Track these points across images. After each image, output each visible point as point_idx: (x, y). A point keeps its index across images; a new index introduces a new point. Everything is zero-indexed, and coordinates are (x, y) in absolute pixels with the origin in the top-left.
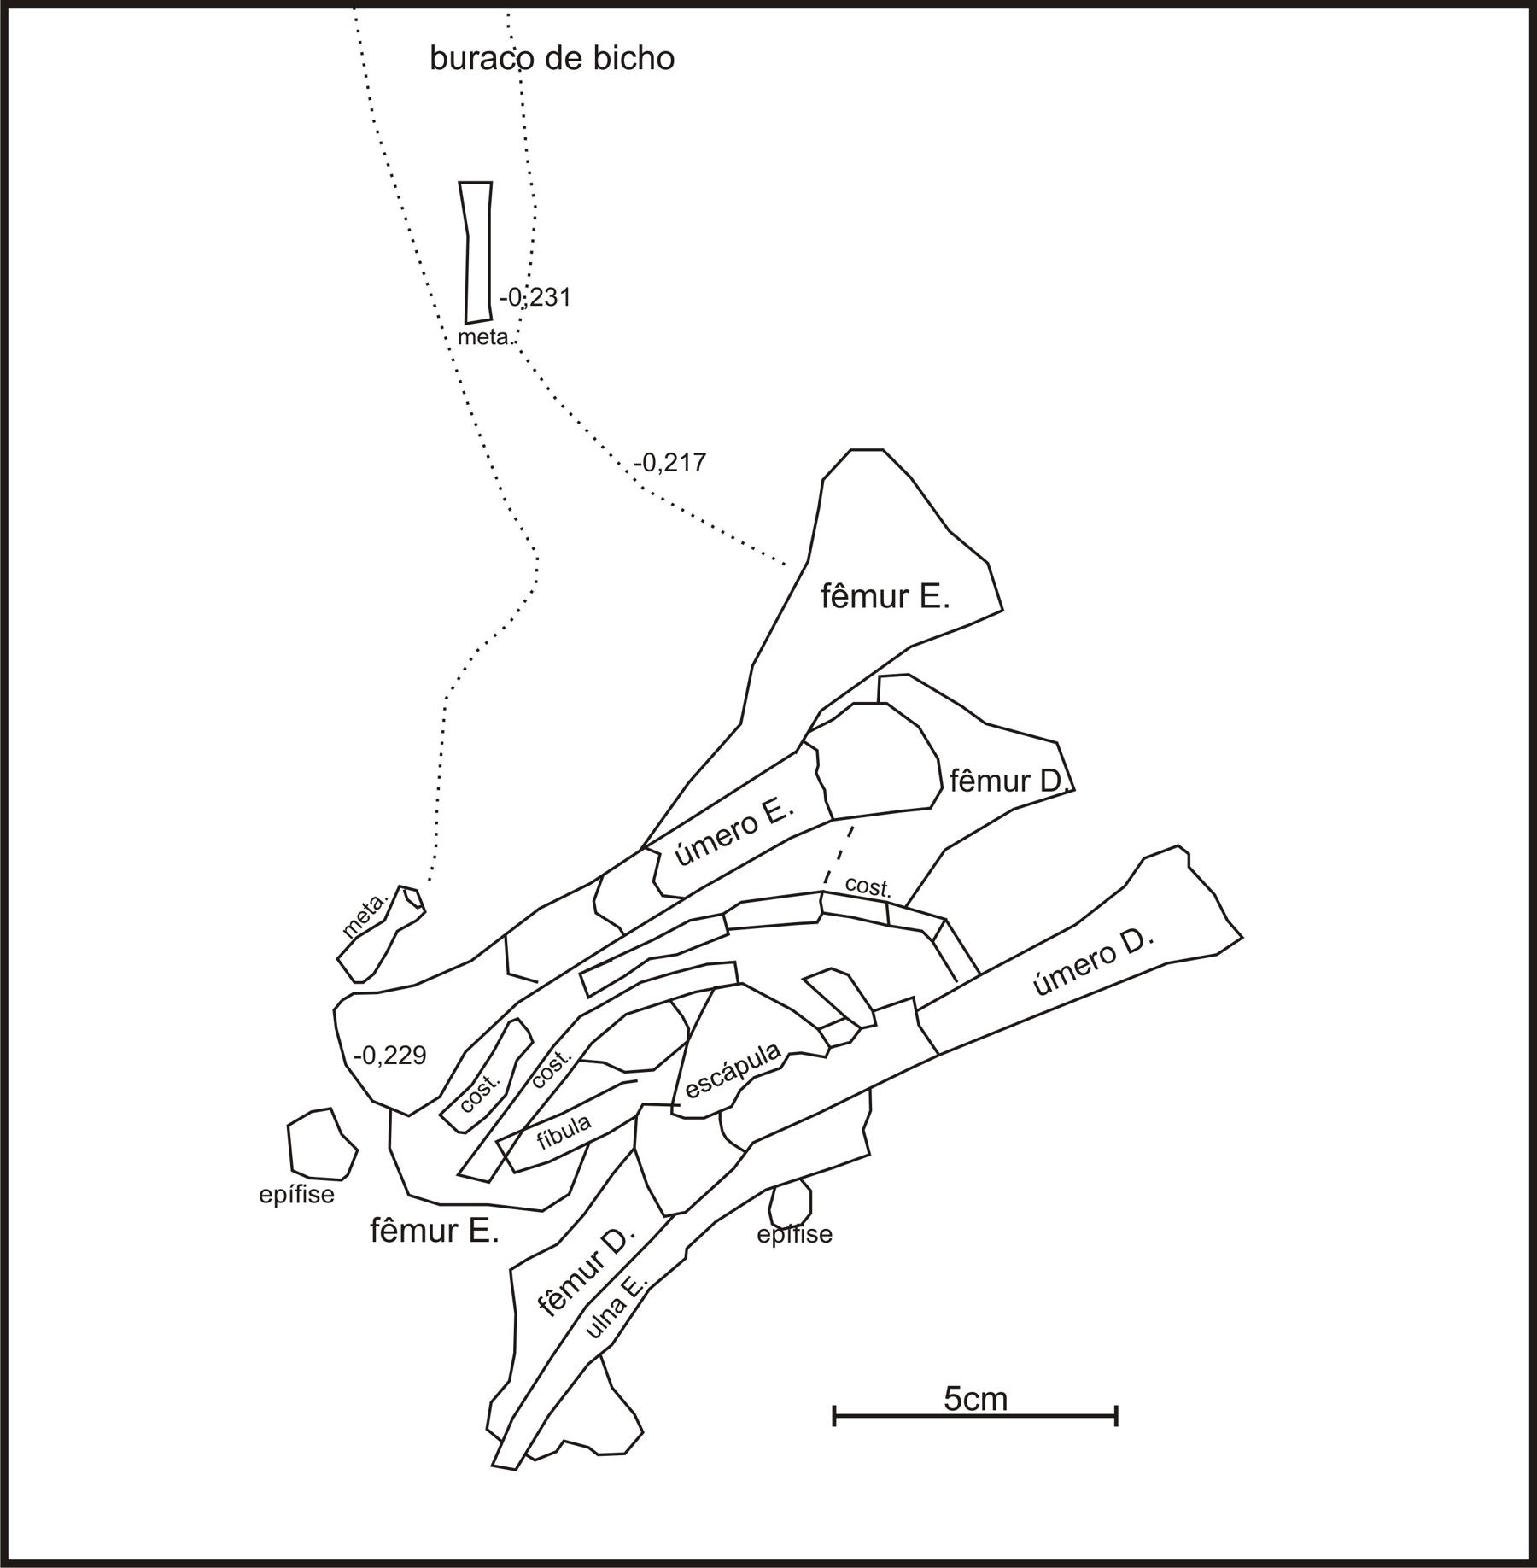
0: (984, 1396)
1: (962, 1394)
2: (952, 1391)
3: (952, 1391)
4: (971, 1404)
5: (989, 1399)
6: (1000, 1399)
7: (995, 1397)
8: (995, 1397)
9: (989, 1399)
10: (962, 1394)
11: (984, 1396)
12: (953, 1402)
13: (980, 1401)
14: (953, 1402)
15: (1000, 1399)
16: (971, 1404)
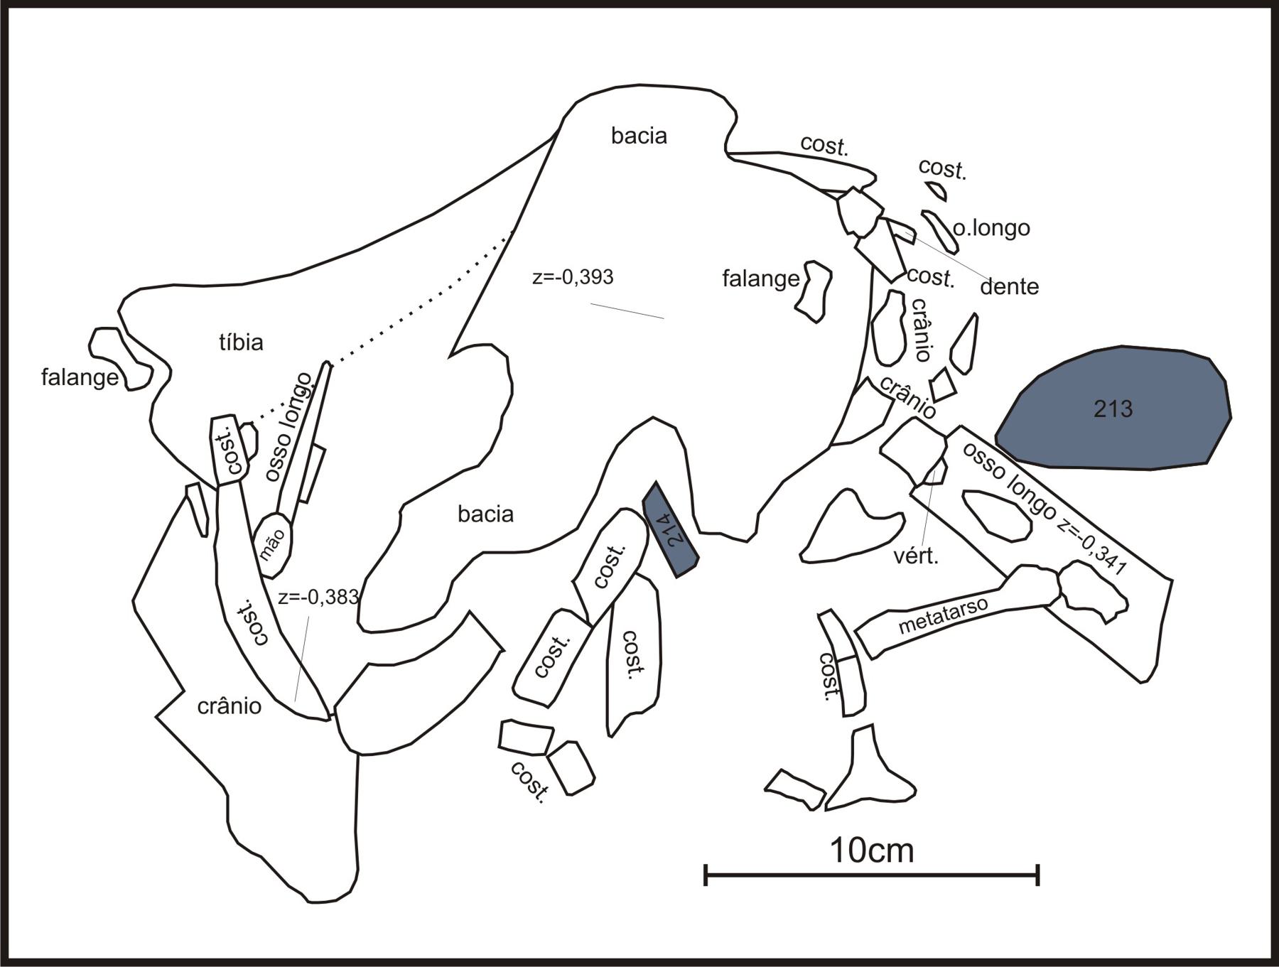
0: (890, 847)
4: (877, 857)
5: (895, 850)
6: (906, 850)
7: (900, 848)
8: (900, 848)
9: (895, 850)
11: (890, 847)
13: (885, 852)
15: (906, 850)
16: (877, 857)
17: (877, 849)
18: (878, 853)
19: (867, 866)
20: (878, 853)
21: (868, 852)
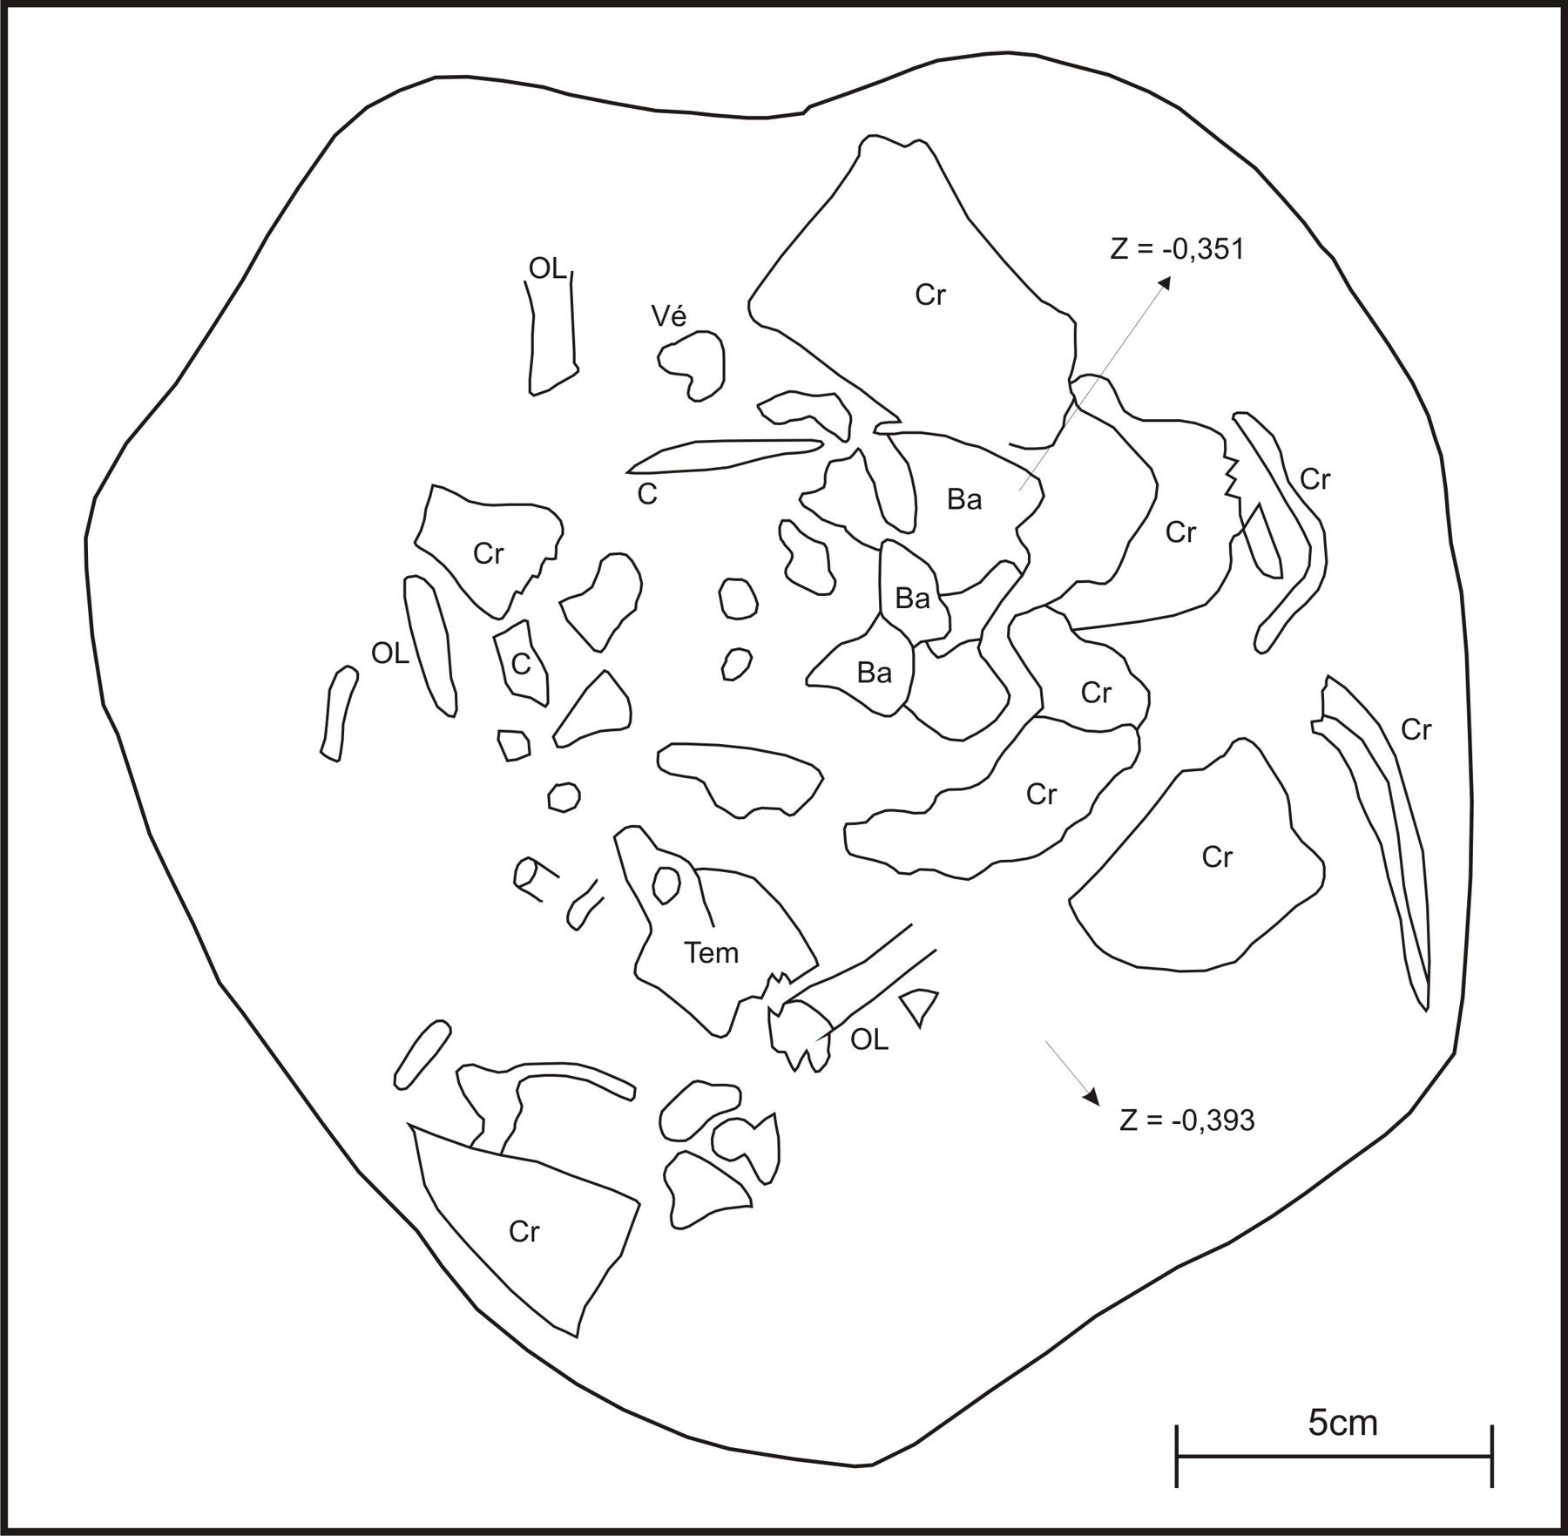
0: (1352, 1419)
1: (1328, 1417)
2: (1317, 1415)
3: (1317, 1415)
4: (1338, 1429)
5: (1358, 1422)
6: (1369, 1422)
7: (1363, 1420)
8: (1363, 1420)
9: (1358, 1422)
10: (1328, 1417)
11: (1352, 1419)
12: (1318, 1426)
13: (1347, 1425)
14: (1318, 1426)
15: (1369, 1422)
16: (1338, 1429)
17: (1338, 1422)
21: (1329, 1426)
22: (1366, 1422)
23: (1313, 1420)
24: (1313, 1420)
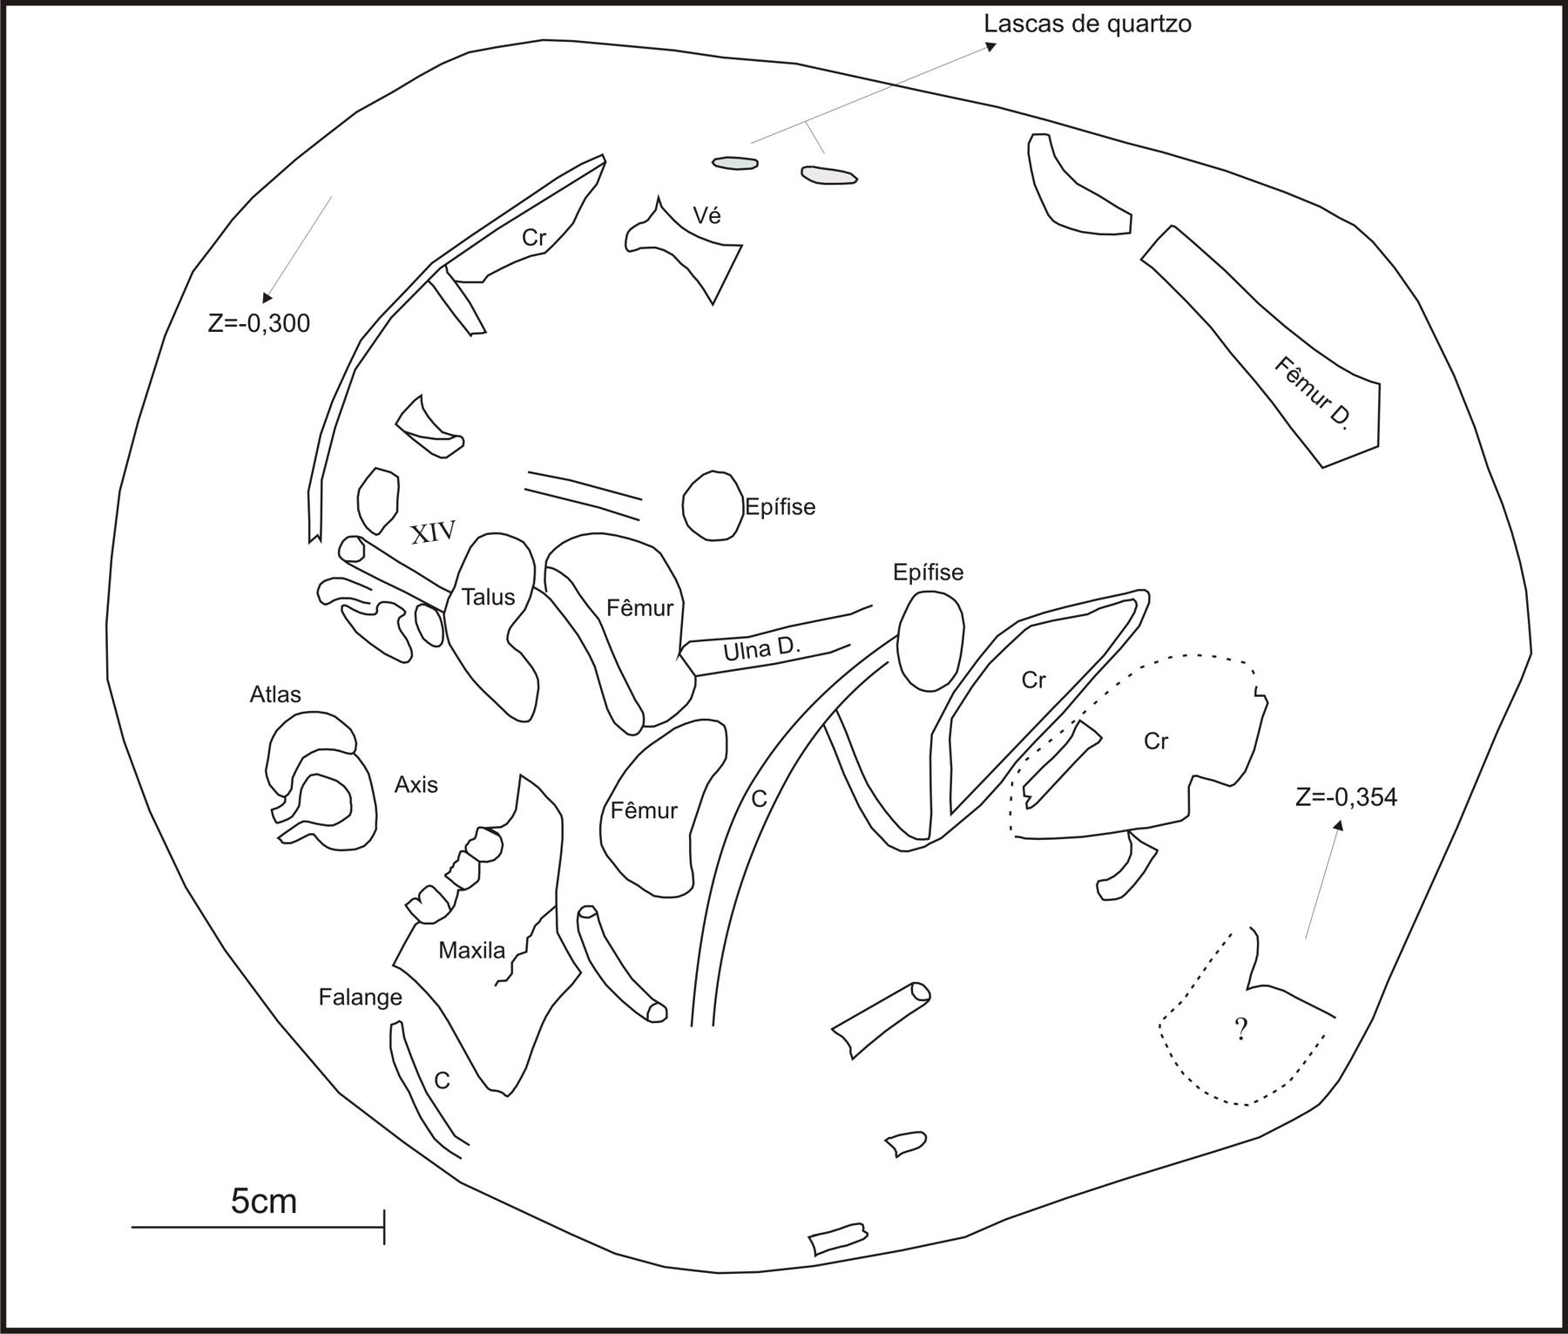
0: (273, 1198)
1: (249, 1195)
2: (239, 1193)
3: (239, 1193)
4: (260, 1208)
5: (278, 1201)
6: (289, 1201)
7: (283, 1199)
8: (283, 1199)
9: (278, 1201)
10: (249, 1195)
11: (273, 1198)
12: (240, 1204)
13: (268, 1203)
14: (240, 1204)
15: (289, 1201)
16: (260, 1208)
17: (259, 1199)
18: (260, 1203)
19: (250, 1217)
20: (260, 1203)
21: (250, 1204)
22: (287, 1200)
23: (235, 1199)
24: (235, 1199)
